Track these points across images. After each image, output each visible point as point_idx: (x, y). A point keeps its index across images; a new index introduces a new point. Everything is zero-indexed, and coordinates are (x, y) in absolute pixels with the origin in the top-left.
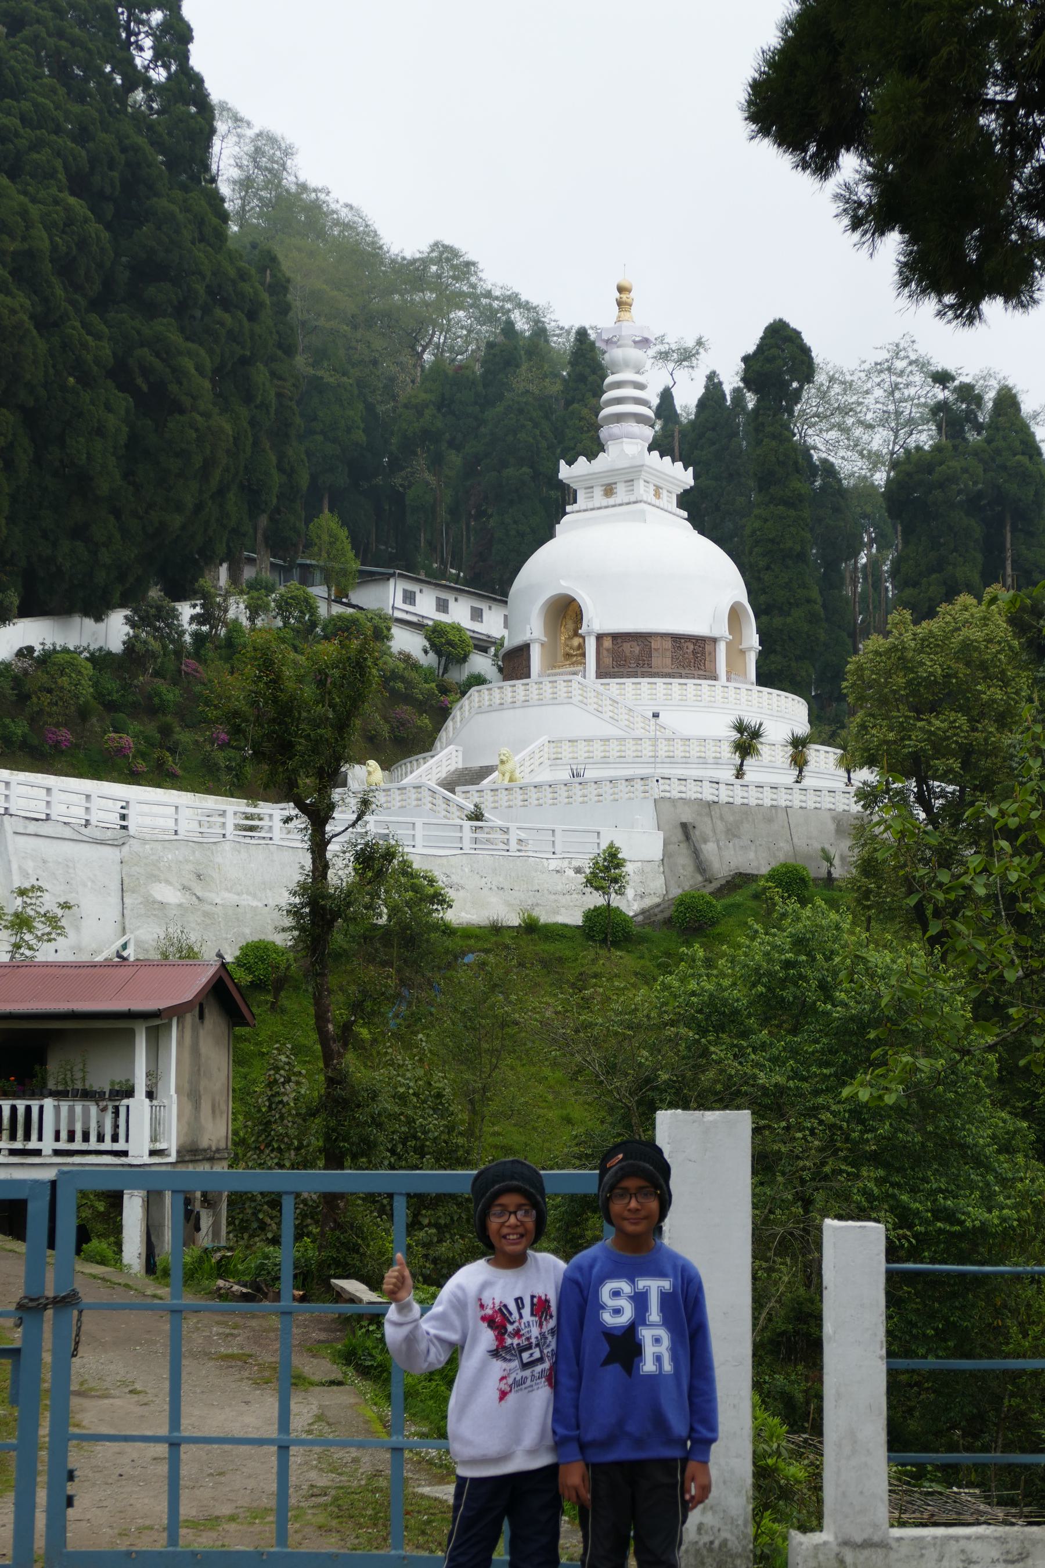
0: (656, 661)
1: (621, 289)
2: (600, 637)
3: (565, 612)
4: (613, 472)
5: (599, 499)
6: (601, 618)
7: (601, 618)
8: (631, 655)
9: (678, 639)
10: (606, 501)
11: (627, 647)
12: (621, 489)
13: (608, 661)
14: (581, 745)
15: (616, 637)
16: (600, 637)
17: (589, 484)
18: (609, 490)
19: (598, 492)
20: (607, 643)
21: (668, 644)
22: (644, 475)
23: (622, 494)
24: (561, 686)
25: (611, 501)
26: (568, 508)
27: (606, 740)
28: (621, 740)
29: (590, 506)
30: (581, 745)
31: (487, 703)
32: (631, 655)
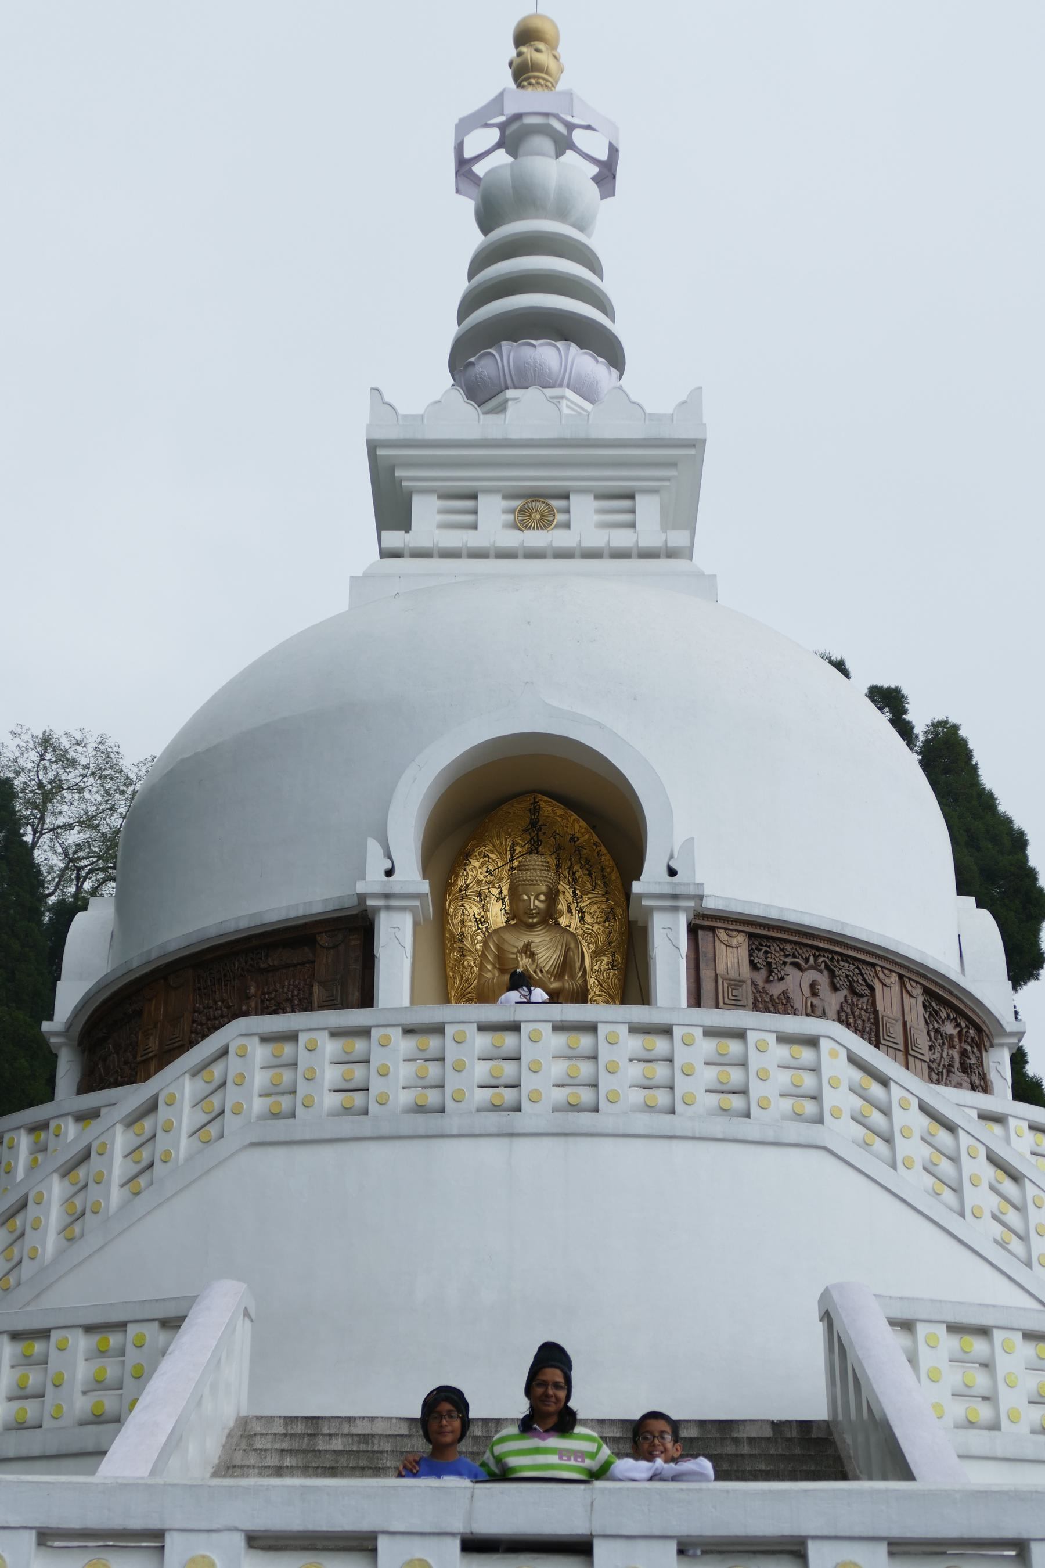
2: (704, 926)
4: (579, 450)
10: (535, 538)
16: (704, 926)
17: (462, 479)
18: (537, 508)
20: (732, 957)
21: (916, 1012)
23: (585, 521)
31: (330, 1101)
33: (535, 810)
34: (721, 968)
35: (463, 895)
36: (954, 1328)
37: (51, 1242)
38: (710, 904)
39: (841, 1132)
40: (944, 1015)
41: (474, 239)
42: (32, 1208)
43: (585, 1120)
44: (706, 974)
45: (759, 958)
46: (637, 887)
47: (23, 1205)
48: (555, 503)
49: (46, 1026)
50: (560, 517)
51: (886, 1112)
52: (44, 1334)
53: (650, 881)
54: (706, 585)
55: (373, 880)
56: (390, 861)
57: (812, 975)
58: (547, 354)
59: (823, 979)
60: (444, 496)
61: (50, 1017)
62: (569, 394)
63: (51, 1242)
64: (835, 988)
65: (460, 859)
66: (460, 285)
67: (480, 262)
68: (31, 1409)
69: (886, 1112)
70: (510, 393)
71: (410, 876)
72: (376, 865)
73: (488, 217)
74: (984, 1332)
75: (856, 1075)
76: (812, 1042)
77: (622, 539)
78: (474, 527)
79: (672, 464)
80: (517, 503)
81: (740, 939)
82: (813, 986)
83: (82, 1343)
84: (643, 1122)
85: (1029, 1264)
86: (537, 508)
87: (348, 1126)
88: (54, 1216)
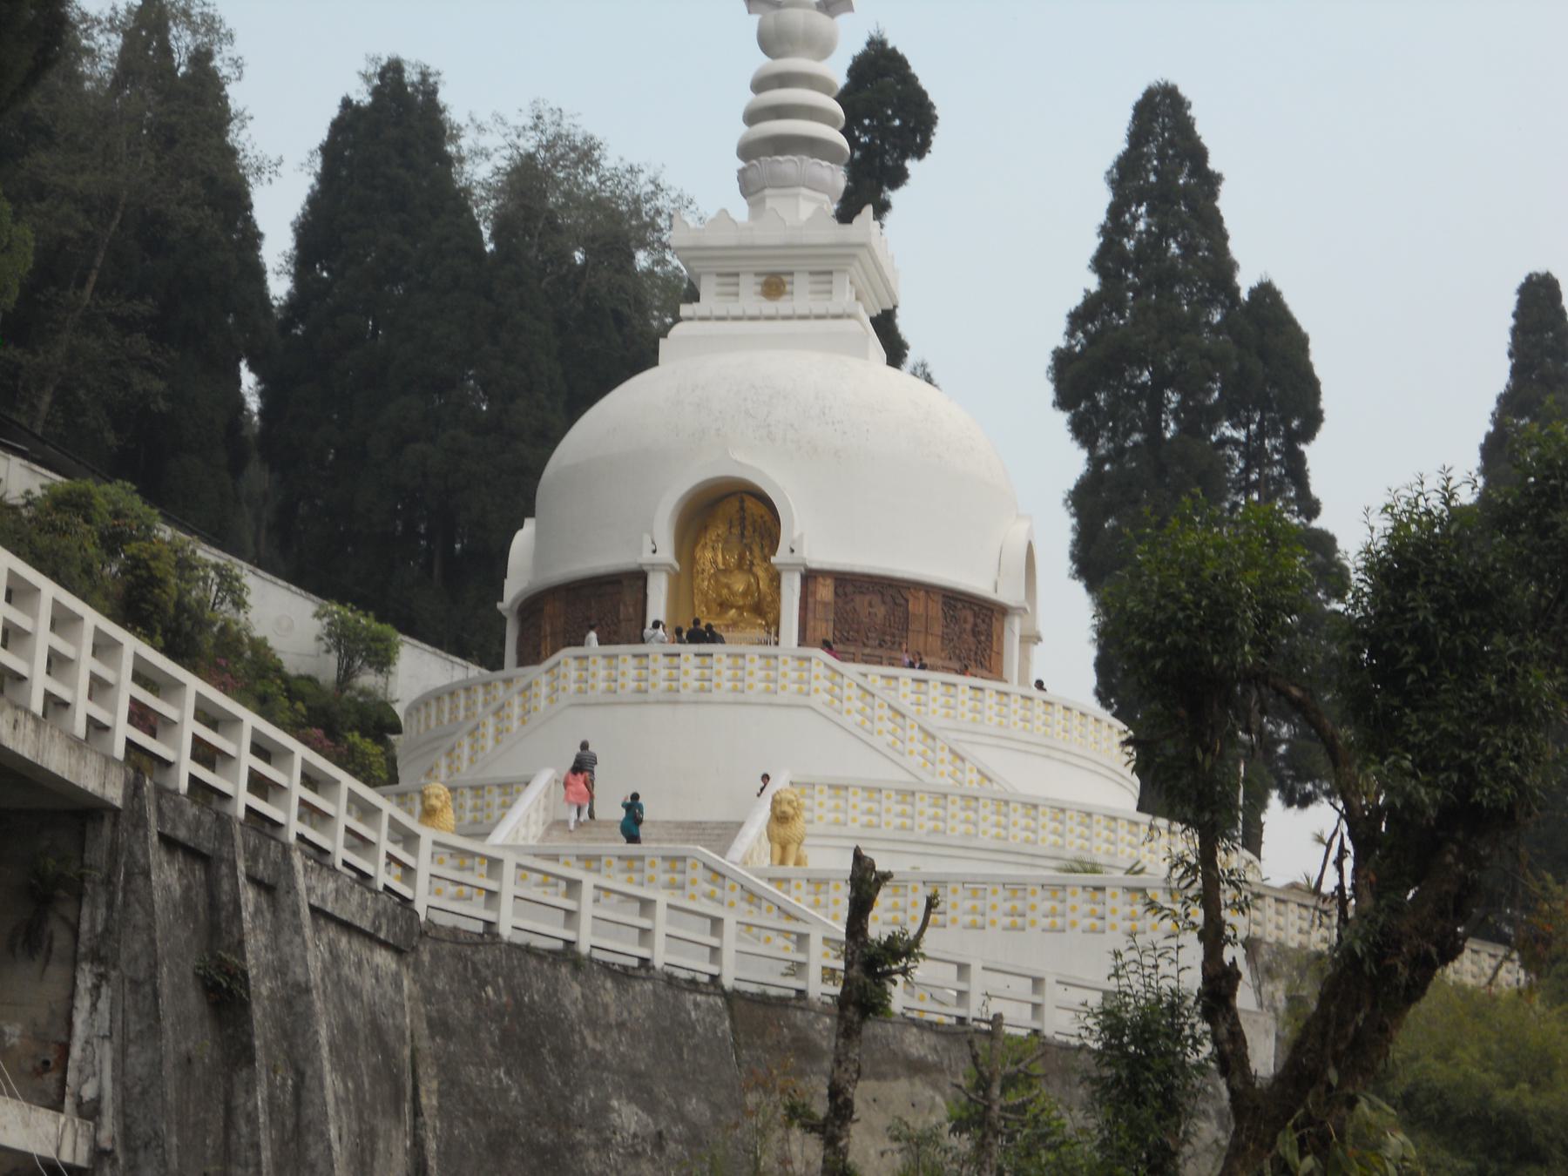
2: (810, 577)
3: (733, 516)
5: (750, 299)
6: (817, 537)
7: (817, 537)
8: (884, 619)
9: (955, 601)
10: (769, 307)
11: (861, 603)
14: (858, 799)
15: (848, 583)
18: (774, 286)
19: (749, 287)
20: (825, 592)
21: (936, 609)
23: (802, 297)
24: (600, 670)
25: (782, 306)
26: (685, 310)
27: (873, 790)
28: (906, 794)
29: (736, 310)
30: (923, 805)
31: (602, 685)
32: (884, 619)
33: (742, 501)
34: (818, 597)
35: (705, 547)
36: (830, 786)
37: (490, 743)
38: (814, 565)
39: (820, 699)
40: (959, 605)
41: (759, 62)
42: (481, 730)
43: (705, 696)
44: (810, 600)
45: (840, 591)
46: (773, 560)
47: (477, 727)
48: (786, 279)
49: (500, 605)
50: (788, 288)
51: (841, 688)
52: (483, 787)
53: (780, 557)
55: (645, 558)
56: (653, 545)
57: (867, 598)
58: (788, 164)
59: (876, 599)
60: (719, 275)
61: (502, 600)
62: (804, 191)
63: (490, 743)
64: (884, 602)
65: (704, 528)
66: (747, 98)
68: (478, 815)
69: (841, 688)
70: (767, 192)
71: (667, 554)
72: (648, 547)
73: (770, 43)
74: (846, 788)
75: (829, 673)
76: (809, 659)
77: (819, 308)
78: (737, 295)
79: (854, 256)
80: (762, 279)
81: (829, 582)
82: (870, 605)
83: (496, 791)
84: (730, 697)
85: (902, 754)
86: (774, 286)
87: (611, 698)
88: (491, 730)
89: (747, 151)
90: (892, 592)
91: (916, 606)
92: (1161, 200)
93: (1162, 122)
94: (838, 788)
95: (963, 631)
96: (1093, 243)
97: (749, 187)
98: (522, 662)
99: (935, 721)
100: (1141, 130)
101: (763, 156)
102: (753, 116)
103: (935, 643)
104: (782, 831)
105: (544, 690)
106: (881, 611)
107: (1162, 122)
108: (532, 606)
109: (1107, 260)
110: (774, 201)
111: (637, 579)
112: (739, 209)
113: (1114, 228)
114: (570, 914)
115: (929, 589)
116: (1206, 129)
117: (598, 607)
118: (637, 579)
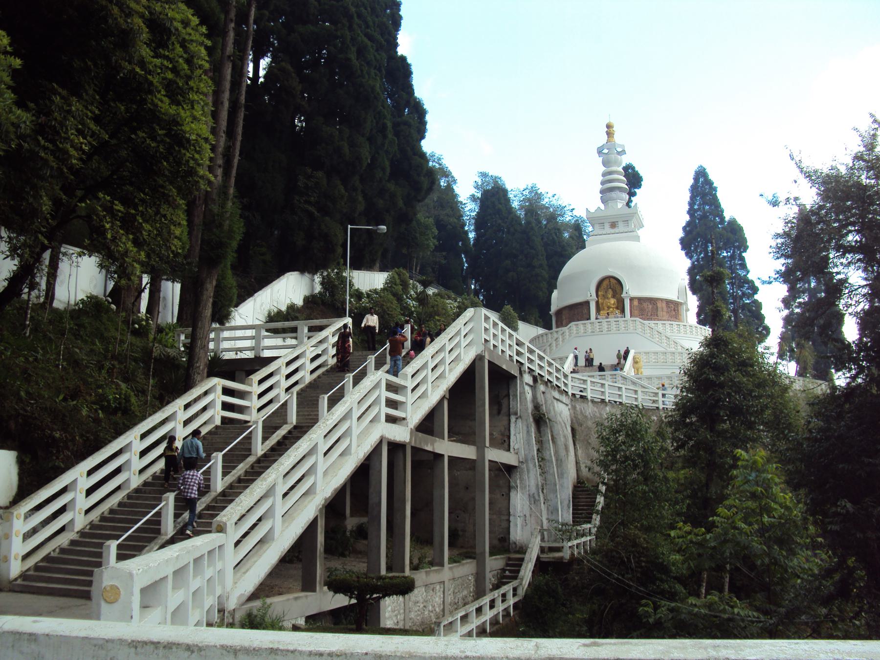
0: (660, 313)
1: (609, 126)
2: (632, 299)
3: (611, 286)
7: (632, 290)
9: (669, 302)
10: (613, 231)
11: (645, 305)
12: (621, 224)
13: (636, 312)
15: (641, 300)
16: (632, 299)
18: (613, 225)
19: (607, 226)
20: (636, 303)
21: (664, 305)
22: (634, 219)
23: (621, 227)
25: (616, 230)
27: (656, 353)
29: (604, 232)
41: (603, 169)
54: (637, 238)
55: (589, 298)
56: (590, 294)
58: (614, 194)
67: (604, 175)
73: (605, 164)
86: (613, 225)
89: (602, 192)
90: (652, 301)
91: (659, 305)
92: (704, 195)
93: (701, 175)
94: (647, 353)
95: (673, 309)
96: (687, 207)
97: (604, 201)
98: (557, 327)
99: (669, 334)
100: (696, 179)
101: (607, 192)
102: (603, 183)
103: (665, 313)
104: (637, 366)
105: (567, 334)
106: (650, 306)
107: (701, 175)
108: (559, 312)
109: (691, 212)
110: (610, 203)
111: (587, 303)
112: (602, 207)
113: (691, 204)
114: (620, 395)
115: (662, 300)
116: (711, 177)
117: (577, 312)
118: (587, 303)
